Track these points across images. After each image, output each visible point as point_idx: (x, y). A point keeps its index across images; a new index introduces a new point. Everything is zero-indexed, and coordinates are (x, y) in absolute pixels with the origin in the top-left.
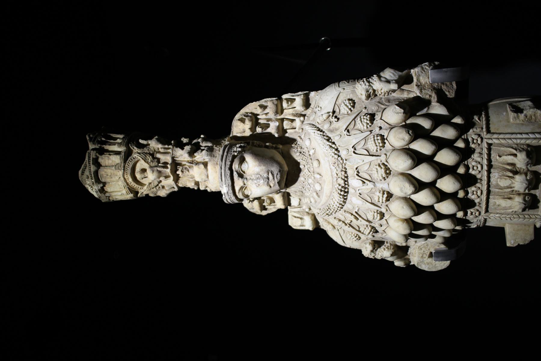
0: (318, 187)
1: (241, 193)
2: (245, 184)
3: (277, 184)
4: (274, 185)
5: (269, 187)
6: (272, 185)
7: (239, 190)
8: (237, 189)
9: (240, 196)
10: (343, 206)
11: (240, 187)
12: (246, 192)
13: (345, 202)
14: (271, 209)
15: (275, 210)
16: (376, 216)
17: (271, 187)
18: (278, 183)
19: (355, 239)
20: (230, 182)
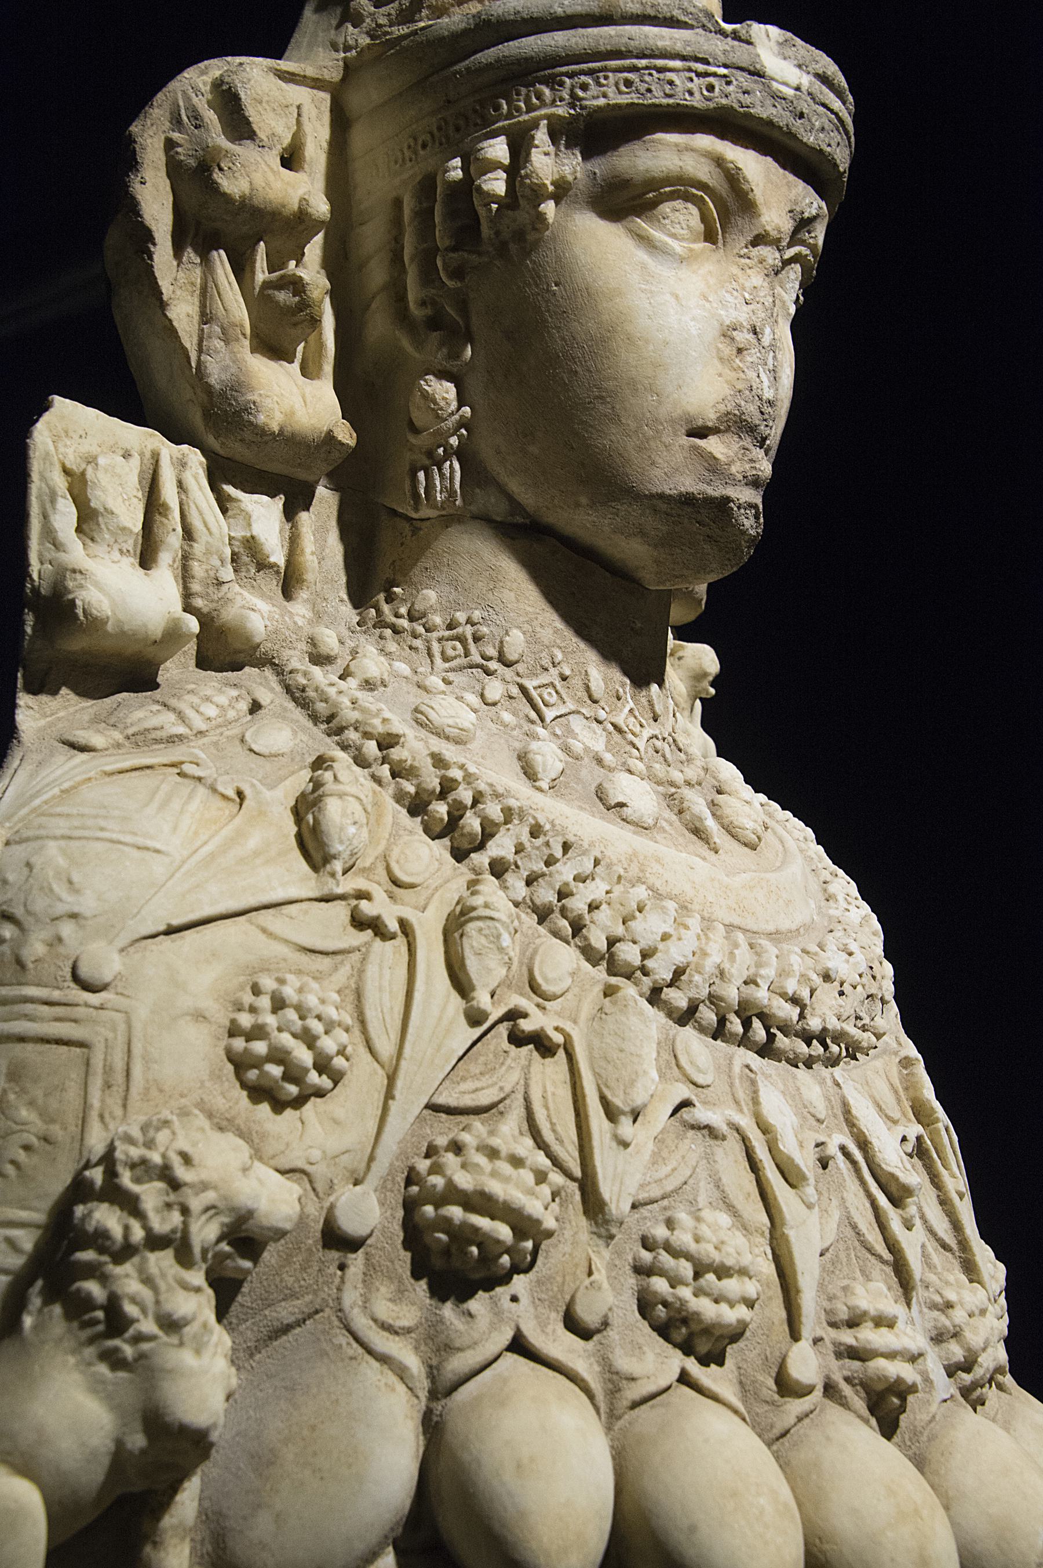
0: (639, 795)
1: (704, 172)
2: (757, 241)
3: (715, 491)
4: (713, 467)
5: (711, 418)
6: (713, 445)
7: (733, 177)
8: (754, 167)
9: (669, 153)
10: (654, 996)
11: (759, 194)
12: (681, 219)
13: (686, 1017)
14: (192, 297)
15: (183, 312)
16: (732, 1286)
17: (701, 432)
18: (727, 500)
19: (304, 1056)
20: (810, 139)
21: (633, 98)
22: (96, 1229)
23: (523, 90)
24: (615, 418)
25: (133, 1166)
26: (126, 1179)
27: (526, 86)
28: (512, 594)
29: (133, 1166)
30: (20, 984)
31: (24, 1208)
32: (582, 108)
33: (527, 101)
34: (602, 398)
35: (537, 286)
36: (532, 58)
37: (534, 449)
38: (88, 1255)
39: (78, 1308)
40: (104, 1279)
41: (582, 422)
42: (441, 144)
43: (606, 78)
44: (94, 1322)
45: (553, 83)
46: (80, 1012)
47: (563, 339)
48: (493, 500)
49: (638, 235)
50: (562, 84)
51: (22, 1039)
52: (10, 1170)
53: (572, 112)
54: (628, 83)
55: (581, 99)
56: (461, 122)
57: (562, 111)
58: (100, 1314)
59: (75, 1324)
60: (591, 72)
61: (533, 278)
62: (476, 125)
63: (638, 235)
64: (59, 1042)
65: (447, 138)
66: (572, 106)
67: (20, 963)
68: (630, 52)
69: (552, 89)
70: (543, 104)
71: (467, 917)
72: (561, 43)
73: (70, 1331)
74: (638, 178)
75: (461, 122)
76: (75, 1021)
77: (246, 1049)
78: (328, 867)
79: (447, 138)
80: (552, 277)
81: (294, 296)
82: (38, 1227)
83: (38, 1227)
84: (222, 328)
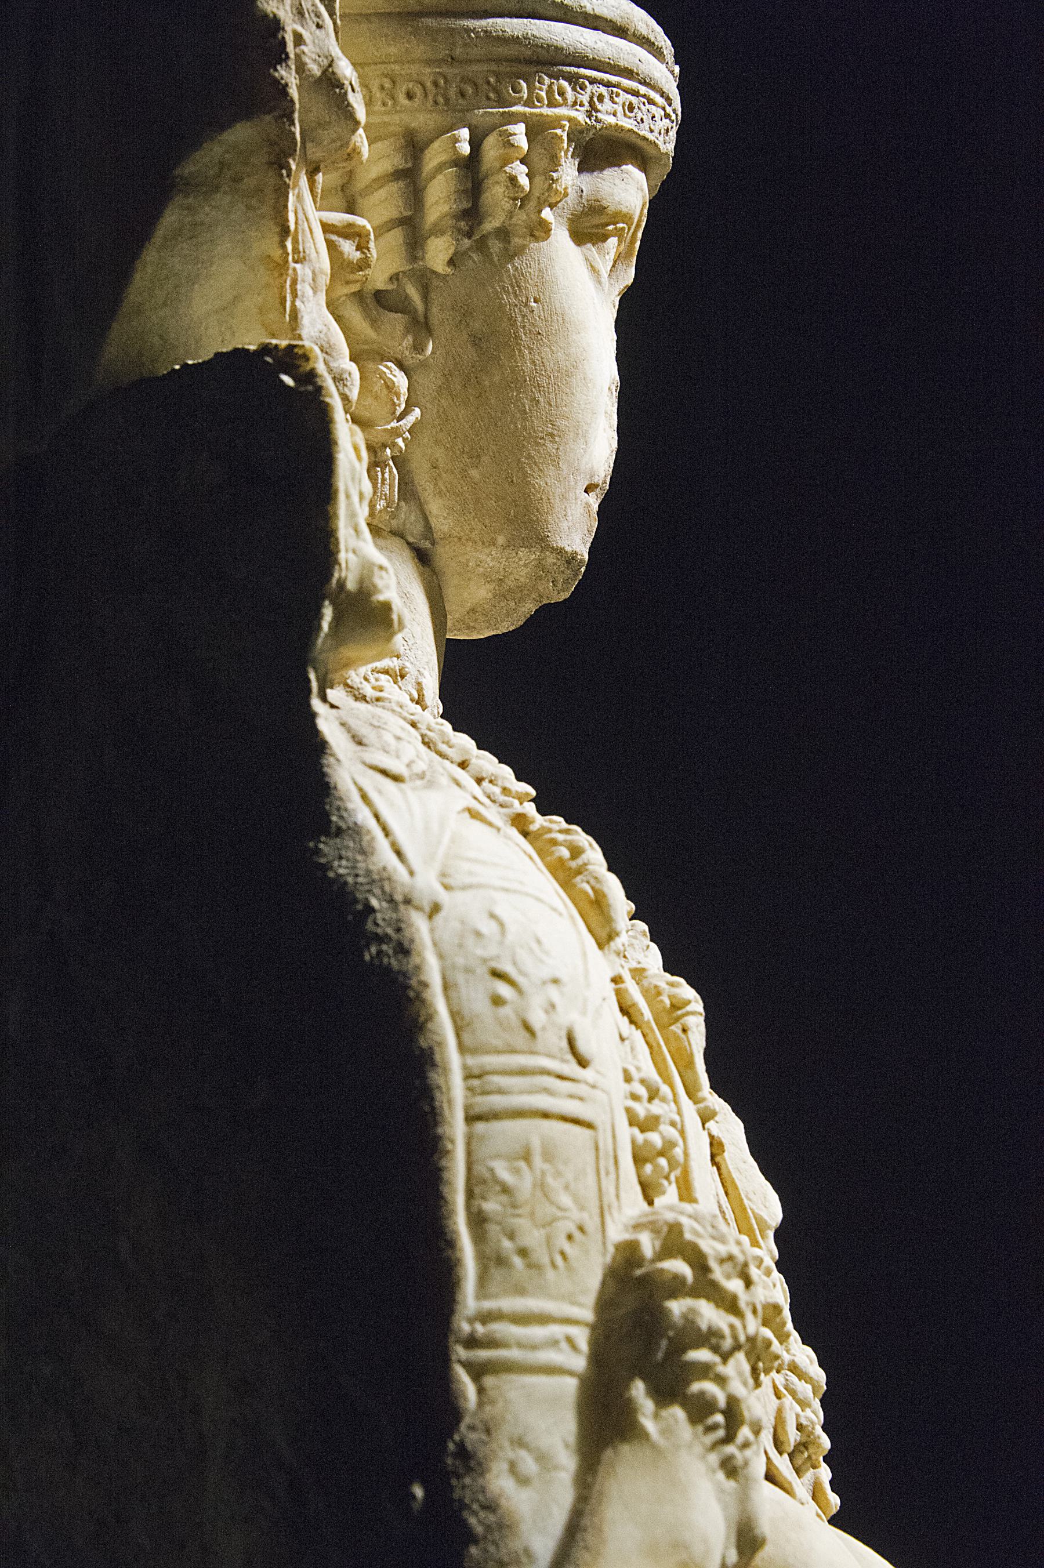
21: (628, 124)
22: (710, 1328)
23: (547, 80)
24: (556, 462)
25: (722, 1261)
26: (718, 1273)
27: (550, 76)
28: (419, 629)
29: (722, 1261)
30: (532, 1053)
31: (574, 1303)
32: (597, 120)
33: (550, 92)
34: (552, 435)
35: (516, 296)
36: (562, 49)
37: (474, 473)
38: (702, 1355)
39: (699, 1410)
40: (721, 1380)
41: (529, 457)
42: (436, 102)
43: (618, 95)
44: (714, 1427)
45: (575, 84)
46: (581, 1089)
47: (533, 363)
48: (413, 518)
49: (592, 266)
50: (583, 88)
51: (546, 1115)
52: (559, 1260)
53: (588, 120)
54: (631, 108)
55: (597, 111)
56: (469, 90)
57: (580, 116)
58: (719, 1418)
59: (700, 1428)
60: (608, 85)
61: (512, 286)
62: (488, 99)
63: (592, 266)
64: (576, 1121)
65: (447, 101)
66: (590, 117)
67: (528, 1028)
68: (638, 74)
69: (574, 89)
70: (565, 103)
71: (684, 1011)
72: (591, 44)
73: (695, 1435)
74: (612, 209)
75: (469, 90)
76: (581, 1099)
77: (646, 1141)
78: (612, 944)
79: (447, 101)
80: (533, 293)
81: (357, 250)
82: (587, 1325)
83: (587, 1325)
84: (314, 273)
